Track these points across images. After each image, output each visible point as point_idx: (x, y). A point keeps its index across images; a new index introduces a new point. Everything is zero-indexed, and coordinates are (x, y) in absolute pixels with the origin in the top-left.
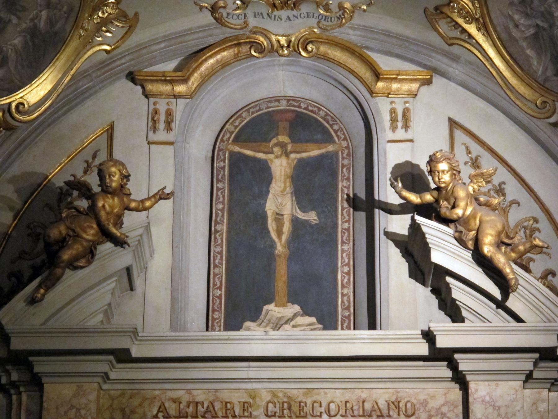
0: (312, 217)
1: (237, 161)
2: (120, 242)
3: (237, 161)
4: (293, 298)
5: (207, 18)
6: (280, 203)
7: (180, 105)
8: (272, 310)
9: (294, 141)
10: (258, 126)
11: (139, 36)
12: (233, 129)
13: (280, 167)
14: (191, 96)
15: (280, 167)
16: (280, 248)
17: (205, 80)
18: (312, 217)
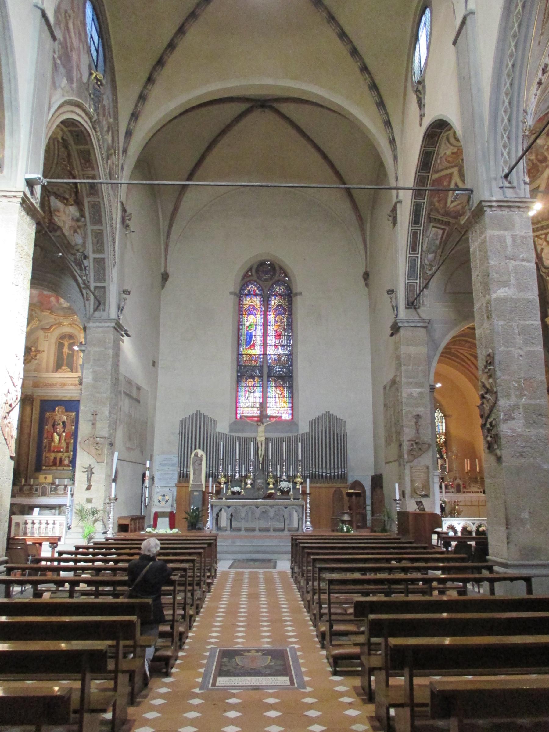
0: (71, 352)
1: (60, 343)
2: (36, 359)
3: (60, 343)
4: (66, 366)
5: (53, 320)
6: (66, 350)
7: (49, 334)
8: (64, 368)
9: (69, 339)
10: (63, 337)
11: (43, 323)
12: (59, 337)
13: (66, 344)
14: (51, 332)
15: (66, 344)
16: (65, 357)
17: (53, 330)
18: (71, 352)
